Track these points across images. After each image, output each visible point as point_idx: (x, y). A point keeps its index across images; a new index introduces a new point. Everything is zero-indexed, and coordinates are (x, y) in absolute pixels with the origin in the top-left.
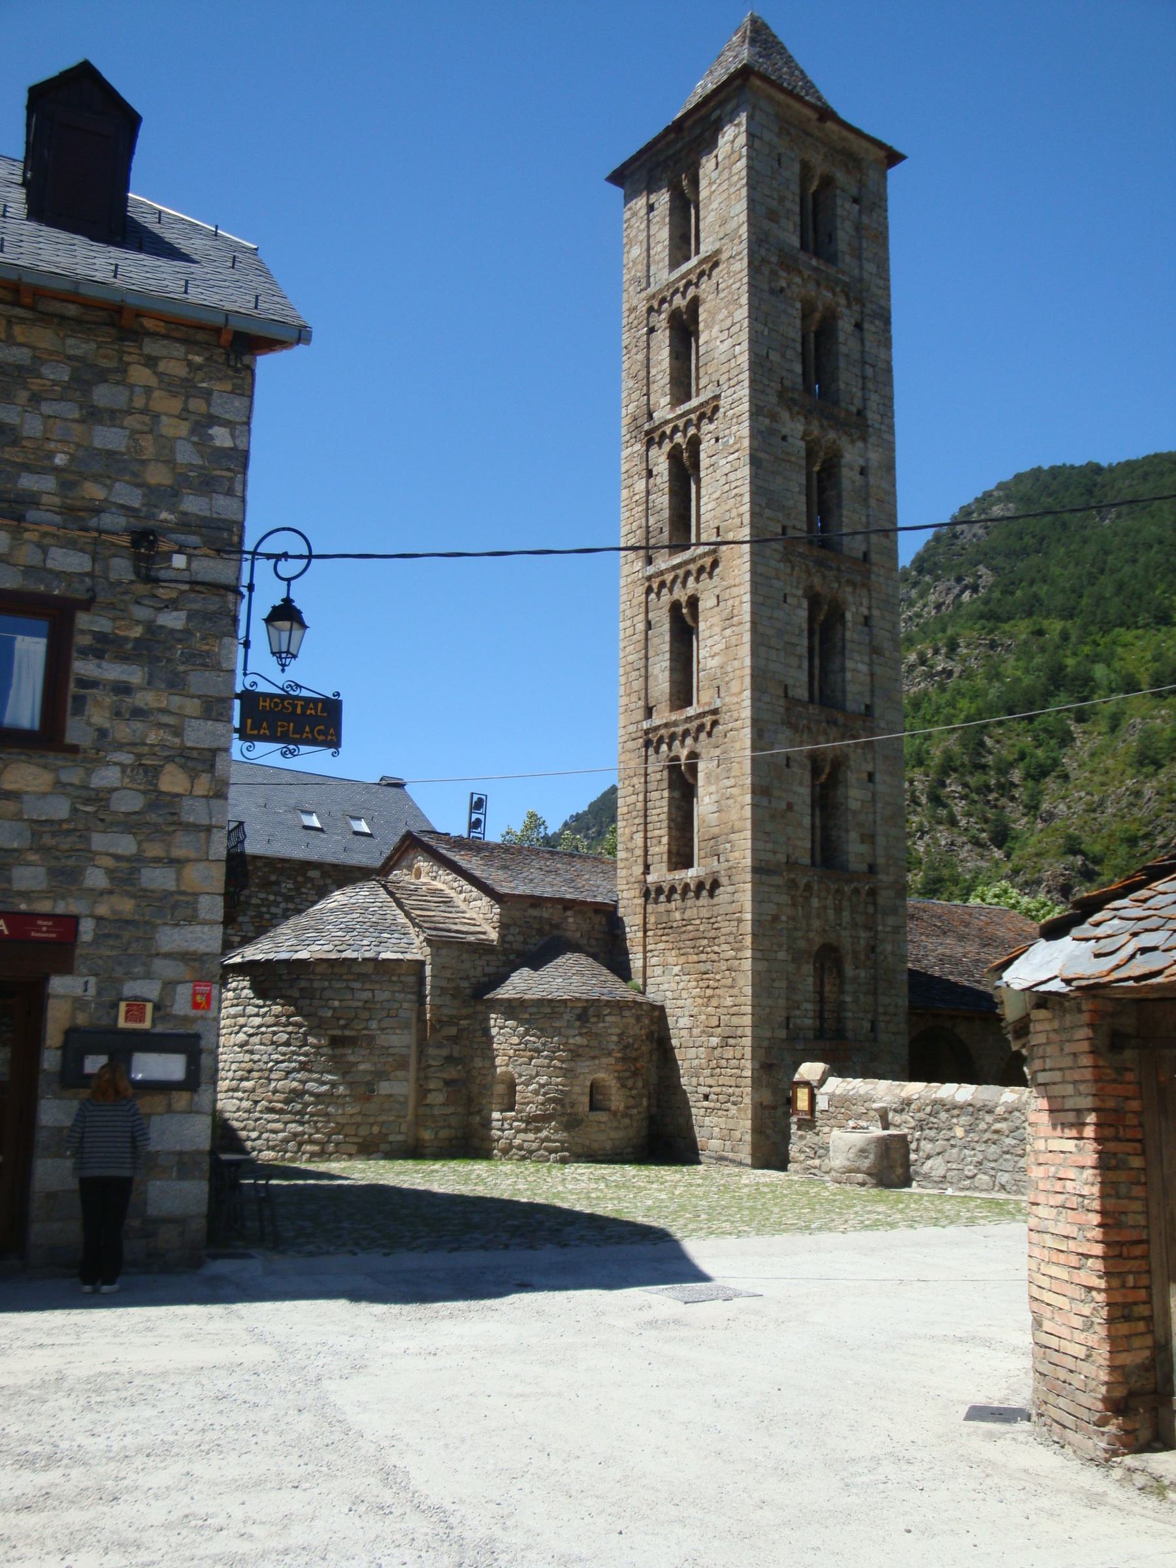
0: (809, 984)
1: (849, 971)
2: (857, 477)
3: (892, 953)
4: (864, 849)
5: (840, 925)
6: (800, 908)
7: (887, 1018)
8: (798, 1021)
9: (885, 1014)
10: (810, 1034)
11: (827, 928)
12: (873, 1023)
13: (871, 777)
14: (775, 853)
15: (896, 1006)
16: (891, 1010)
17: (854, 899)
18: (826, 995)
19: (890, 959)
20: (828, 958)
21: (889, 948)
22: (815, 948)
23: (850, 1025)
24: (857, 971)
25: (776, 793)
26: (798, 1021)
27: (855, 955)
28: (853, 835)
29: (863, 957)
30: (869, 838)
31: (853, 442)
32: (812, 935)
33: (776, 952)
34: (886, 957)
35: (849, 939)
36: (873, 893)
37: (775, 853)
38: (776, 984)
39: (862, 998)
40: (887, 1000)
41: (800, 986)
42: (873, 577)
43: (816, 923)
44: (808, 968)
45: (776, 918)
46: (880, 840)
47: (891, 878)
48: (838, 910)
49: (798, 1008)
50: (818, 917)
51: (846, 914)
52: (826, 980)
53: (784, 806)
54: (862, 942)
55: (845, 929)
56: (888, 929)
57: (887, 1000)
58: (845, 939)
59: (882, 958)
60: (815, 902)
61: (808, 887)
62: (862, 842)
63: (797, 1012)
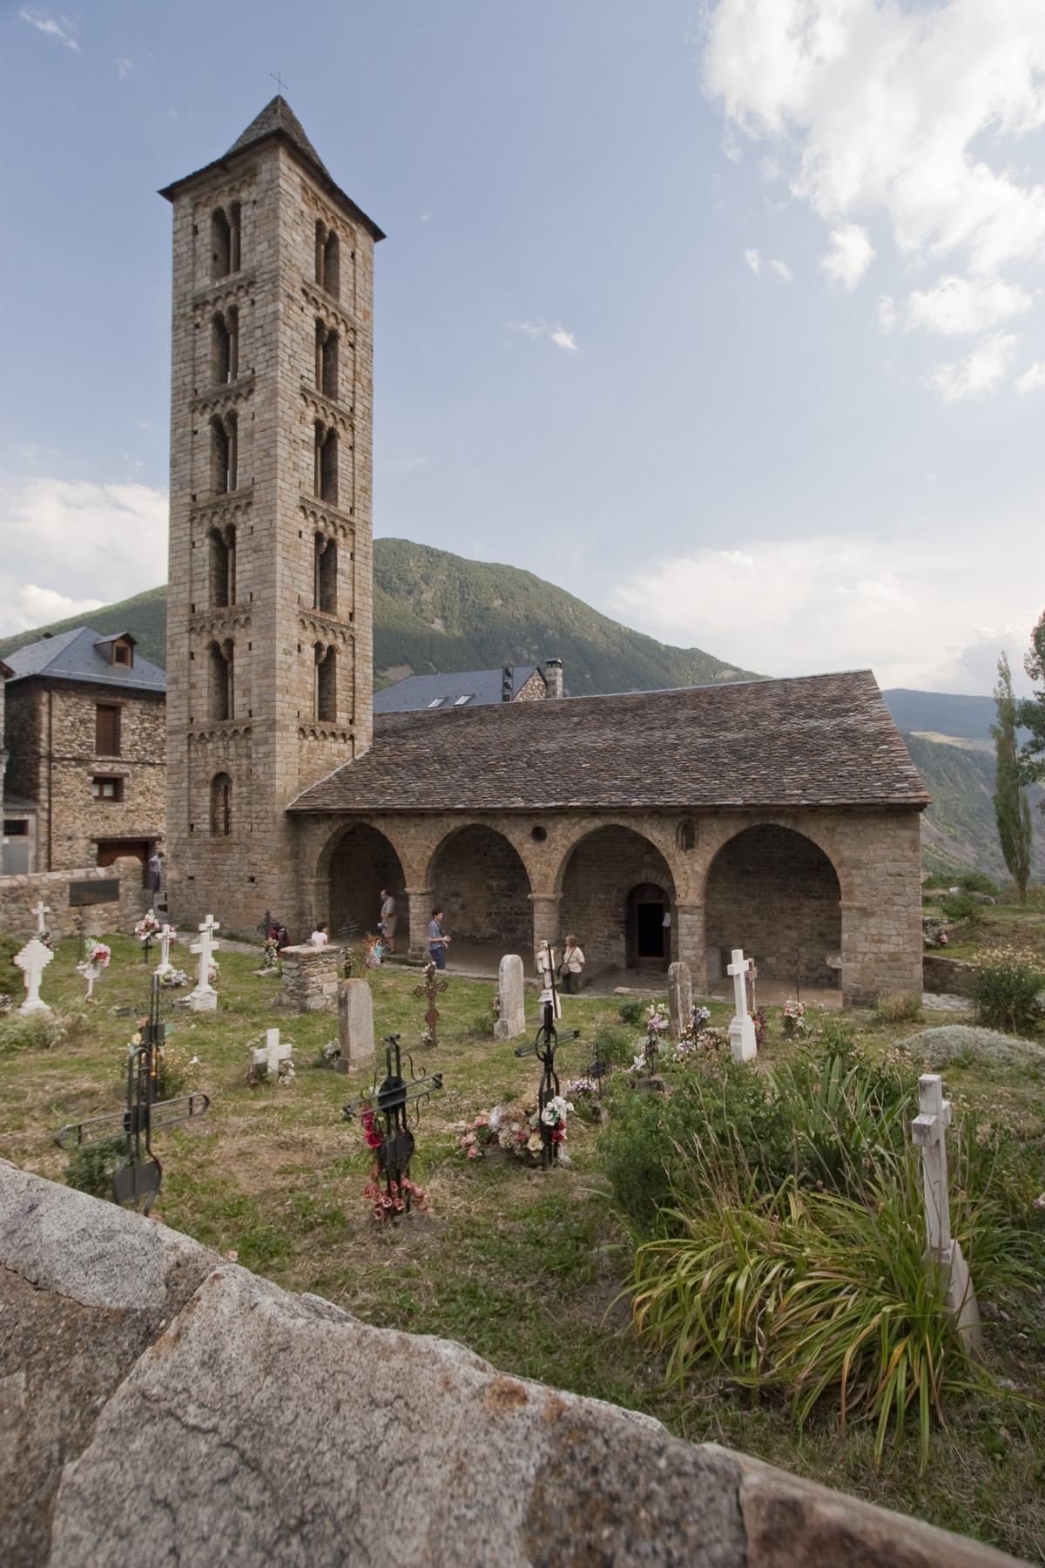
0: (206, 802)
1: (235, 789)
4: (245, 700)
10: (208, 834)
16: (262, 814)
20: (221, 781)
21: (260, 769)
23: (234, 827)
28: (237, 693)
36: (248, 730)
40: (259, 808)
43: (211, 760)
44: (207, 791)
45: (181, 762)
46: (255, 691)
48: (226, 748)
51: (232, 750)
53: (186, 686)
57: (259, 808)
58: (232, 769)
60: (210, 746)
61: (202, 735)
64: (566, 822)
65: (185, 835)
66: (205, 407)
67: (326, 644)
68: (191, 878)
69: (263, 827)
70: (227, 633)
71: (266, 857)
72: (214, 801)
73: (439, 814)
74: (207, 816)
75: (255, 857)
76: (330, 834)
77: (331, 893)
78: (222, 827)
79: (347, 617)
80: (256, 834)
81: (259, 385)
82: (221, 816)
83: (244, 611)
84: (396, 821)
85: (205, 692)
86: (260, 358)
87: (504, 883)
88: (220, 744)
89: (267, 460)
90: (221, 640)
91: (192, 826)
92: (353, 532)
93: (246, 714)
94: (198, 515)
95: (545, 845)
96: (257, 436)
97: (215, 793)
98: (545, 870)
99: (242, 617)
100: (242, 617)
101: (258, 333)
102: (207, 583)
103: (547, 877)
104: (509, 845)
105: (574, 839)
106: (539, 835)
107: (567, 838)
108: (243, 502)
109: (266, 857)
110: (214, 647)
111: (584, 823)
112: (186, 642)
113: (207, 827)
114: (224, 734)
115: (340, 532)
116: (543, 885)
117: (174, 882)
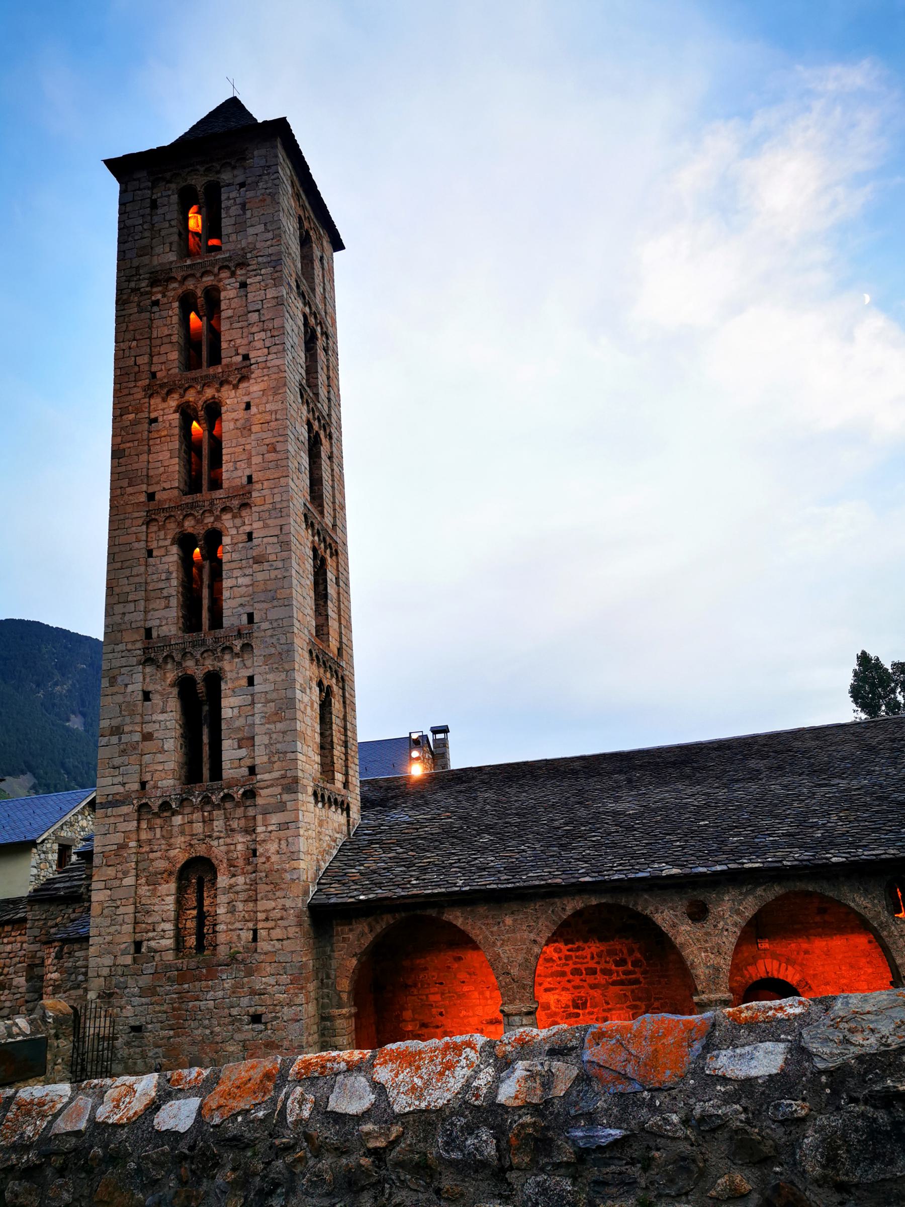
1: (223, 881)
2: (241, 414)
3: (278, 852)
5: (210, 836)
6: (158, 831)
7: (271, 924)
8: (153, 944)
9: (267, 919)
11: (192, 842)
12: (255, 932)
13: (251, 681)
14: (124, 784)
15: (284, 908)
16: (277, 914)
17: (228, 805)
18: (205, 909)
19: (274, 858)
21: (273, 847)
22: (179, 866)
24: (234, 879)
25: (127, 729)
26: (153, 944)
27: (231, 864)
29: (241, 862)
30: (247, 741)
31: (236, 387)
32: (172, 853)
33: (121, 879)
34: (268, 858)
35: (223, 848)
36: (251, 794)
37: (124, 784)
38: (121, 910)
39: (240, 906)
41: (156, 908)
42: (254, 494)
43: (180, 840)
45: (123, 846)
47: (276, 775)
48: (208, 822)
49: (154, 930)
50: (182, 833)
51: (219, 824)
52: (205, 894)
53: (137, 737)
54: (240, 847)
55: (219, 838)
56: (270, 828)
58: (218, 850)
59: (263, 859)
60: (178, 820)
62: (240, 747)
63: (151, 934)
64: (734, 892)
65: (128, 960)
66: (169, 393)
67: (326, 683)
68: (137, 1029)
69: (277, 933)
70: (209, 664)
71: (285, 979)
72: (179, 902)
73: (548, 893)
74: (169, 926)
75: (258, 983)
76: (370, 937)
77: (357, 1029)
78: (192, 941)
79: (336, 652)
80: (263, 946)
81: (257, 373)
82: (191, 924)
83: (240, 635)
84: (482, 910)
85: (170, 745)
86: (258, 344)
87: (566, 998)
88: (197, 816)
89: (271, 456)
90: (199, 674)
91: (138, 945)
92: (337, 554)
93: (245, 771)
94: (161, 517)
95: (708, 926)
96: (255, 428)
97: (181, 891)
98: (714, 960)
99: (238, 644)
100: (238, 644)
101: (254, 317)
102: (174, 602)
103: (717, 969)
104: (658, 928)
105: (748, 914)
106: (698, 913)
107: (738, 913)
108: (236, 503)
109: (285, 979)
110: (185, 685)
111: (759, 891)
112: (140, 677)
113: (169, 942)
114: (206, 801)
115: (328, 551)
116: (713, 980)
117: (100, 1038)
